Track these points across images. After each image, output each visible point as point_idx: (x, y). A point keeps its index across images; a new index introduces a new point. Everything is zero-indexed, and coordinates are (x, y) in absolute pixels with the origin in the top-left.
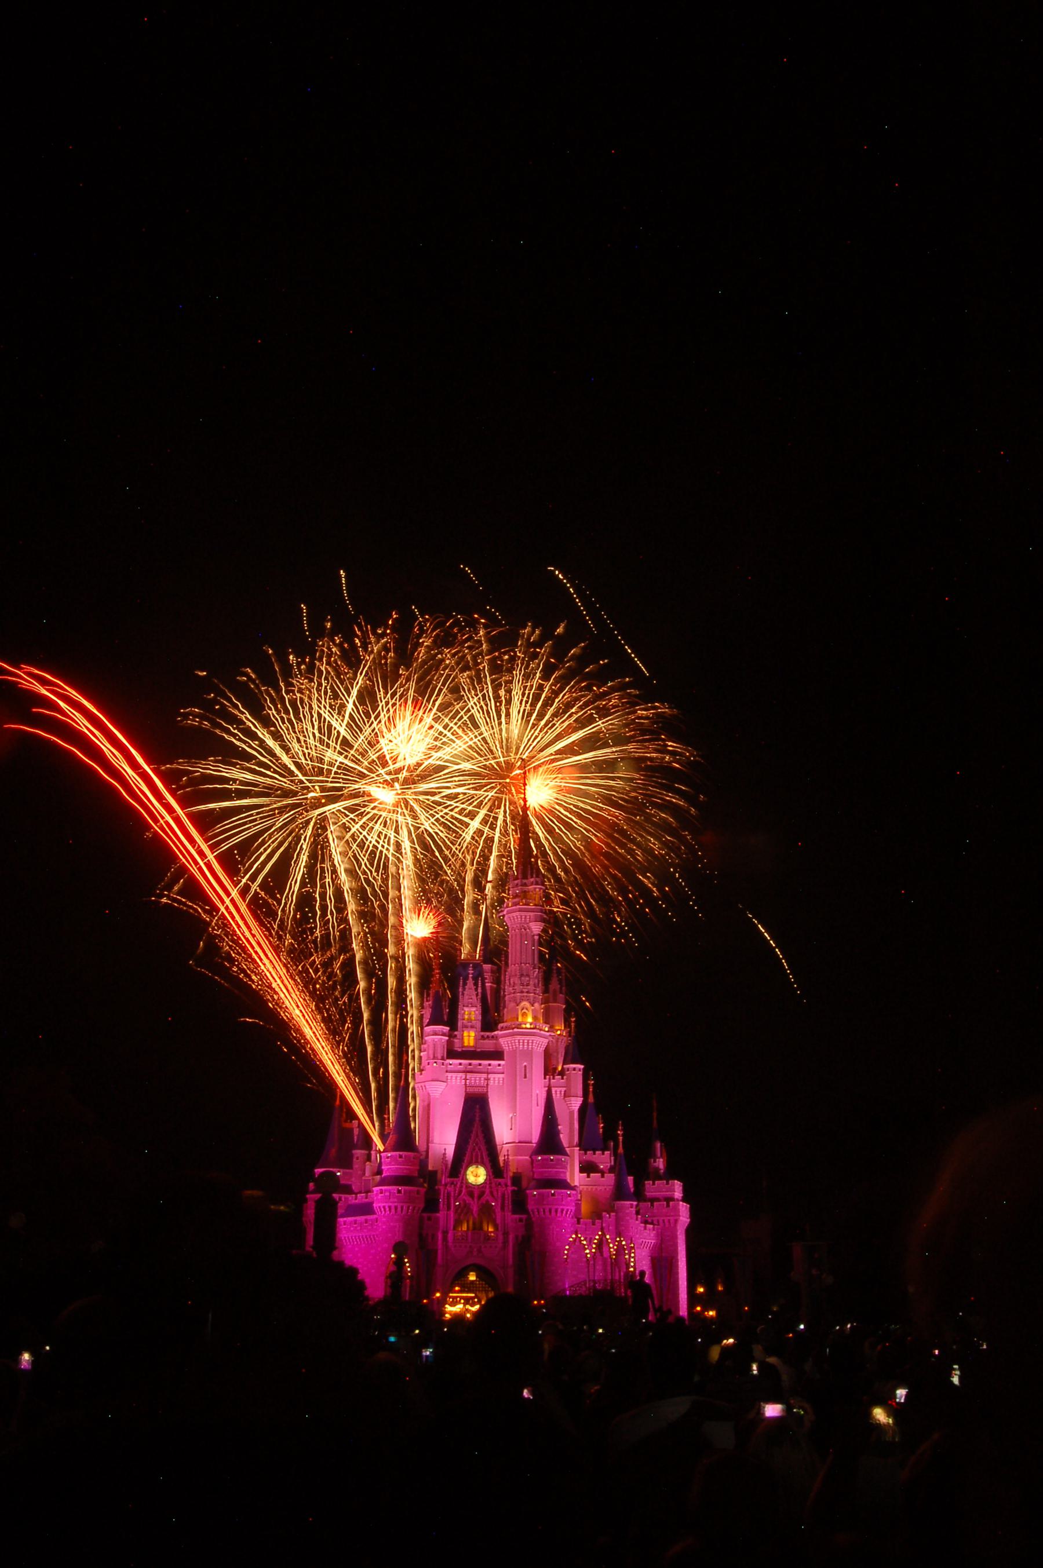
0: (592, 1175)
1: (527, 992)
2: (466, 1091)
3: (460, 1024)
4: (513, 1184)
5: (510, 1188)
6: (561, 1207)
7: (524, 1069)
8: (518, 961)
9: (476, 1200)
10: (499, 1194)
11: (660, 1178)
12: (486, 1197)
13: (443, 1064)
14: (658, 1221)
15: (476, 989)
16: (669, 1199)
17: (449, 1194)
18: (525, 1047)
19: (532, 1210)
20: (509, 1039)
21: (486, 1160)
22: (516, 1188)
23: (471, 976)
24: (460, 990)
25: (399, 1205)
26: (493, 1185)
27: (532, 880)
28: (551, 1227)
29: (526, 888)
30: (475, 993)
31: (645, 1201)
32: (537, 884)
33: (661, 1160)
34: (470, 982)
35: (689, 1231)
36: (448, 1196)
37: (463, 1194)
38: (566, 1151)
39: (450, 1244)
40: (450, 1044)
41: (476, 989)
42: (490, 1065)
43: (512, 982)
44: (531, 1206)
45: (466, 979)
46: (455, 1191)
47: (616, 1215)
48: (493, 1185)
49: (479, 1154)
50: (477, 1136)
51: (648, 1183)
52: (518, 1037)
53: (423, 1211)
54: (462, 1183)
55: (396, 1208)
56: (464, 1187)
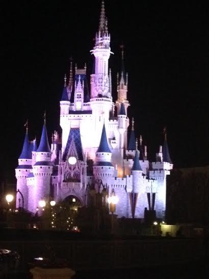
0: (129, 160)
12: (77, 169)
17: (61, 168)
21: (77, 154)
24: (75, 86)
27: (105, 37)
34: (79, 83)
44: (94, 173)
53: (52, 175)
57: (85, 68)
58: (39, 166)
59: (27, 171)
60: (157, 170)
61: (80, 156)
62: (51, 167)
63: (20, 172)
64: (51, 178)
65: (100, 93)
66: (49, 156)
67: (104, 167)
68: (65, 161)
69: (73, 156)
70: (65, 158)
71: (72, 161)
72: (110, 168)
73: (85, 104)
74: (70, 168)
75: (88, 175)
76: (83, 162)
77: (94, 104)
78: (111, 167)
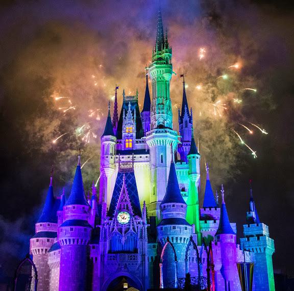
0: (208, 221)
1: (163, 113)
3: (123, 134)
4: (148, 223)
5: (146, 226)
6: (180, 236)
7: (160, 157)
9: (123, 234)
10: (139, 230)
11: (253, 222)
13: (112, 158)
14: (253, 249)
15: (133, 115)
16: (259, 236)
17: (106, 230)
20: (152, 140)
21: (130, 207)
22: (149, 225)
23: (130, 108)
24: (124, 116)
25: (71, 238)
27: (164, 51)
29: (160, 56)
31: (244, 237)
32: (166, 52)
33: (253, 212)
35: (275, 257)
38: (183, 200)
39: (106, 263)
40: (118, 146)
41: (133, 115)
42: (141, 157)
50: (124, 192)
51: (245, 226)
52: (157, 139)
54: (114, 223)
55: (70, 240)
58: (68, 228)
59: (48, 240)
60: (252, 236)
61: (136, 209)
62: (90, 230)
63: (38, 243)
66: (85, 212)
67: (177, 226)
68: (111, 219)
70: (112, 214)
71: (124, 218)
72: (186, 228)
75: (149, 242)
76: (141, 221)
77: (151, 140)
78: (188, 227)
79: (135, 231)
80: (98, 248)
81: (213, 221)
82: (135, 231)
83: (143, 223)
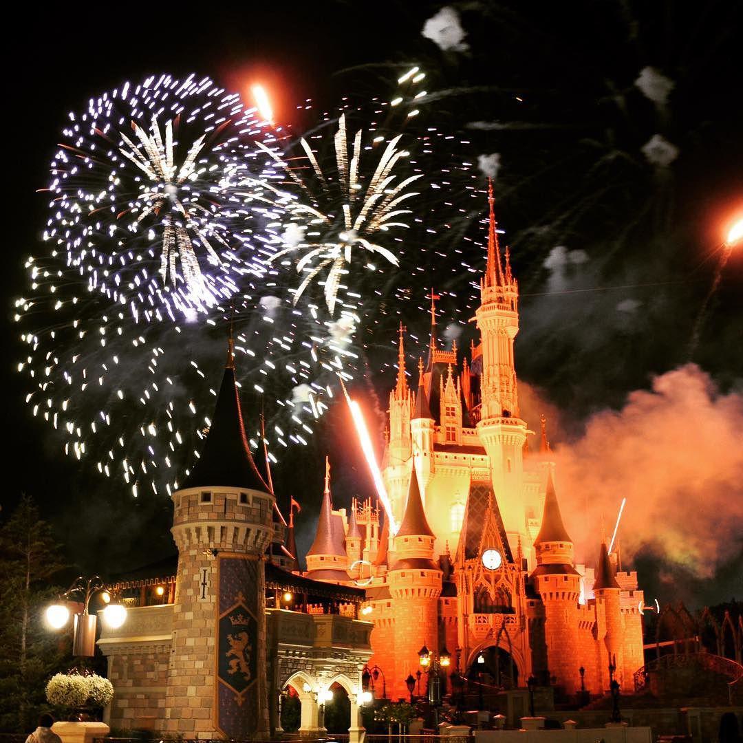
2: (471, 479)
8: (496, 361)
12: (502, 580)
15: (456, 387)
18: (509, 442)
19: (545, 594)
24: (442, 387)
26: (508, 570)
27: (509, 287)
28: (565, 610)
30: (455, 391)
32: (512, 290)
34: (450, 379)
36: (466, 580)
37: (480, 577)
41: (456, 387)
43: (491, 382)
44: (543, 588)
45: (446, 376)
46: (473, 575)
47: (605, 602)
48: (508, 570)
49: (493, 539)
55: (419, 590)
56: (481, 571)
57: (455, 349)
64: (439, 602)
65: (505, 408)
69: (491, 548)
73: (466, 430)
74: (488, 579)
79: (508, 579)
80: (455, 603)
81: (626, 573)
82: (508, 579)
83: (520, 571)
